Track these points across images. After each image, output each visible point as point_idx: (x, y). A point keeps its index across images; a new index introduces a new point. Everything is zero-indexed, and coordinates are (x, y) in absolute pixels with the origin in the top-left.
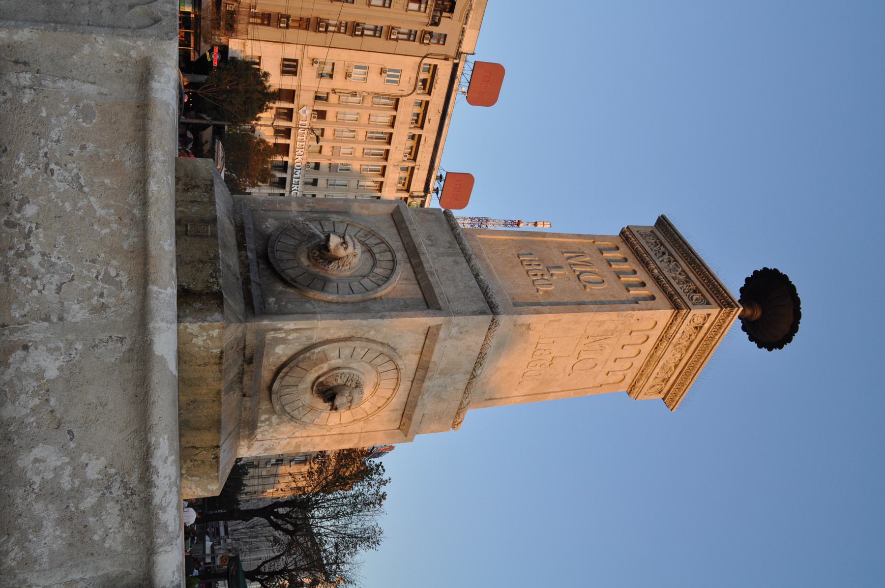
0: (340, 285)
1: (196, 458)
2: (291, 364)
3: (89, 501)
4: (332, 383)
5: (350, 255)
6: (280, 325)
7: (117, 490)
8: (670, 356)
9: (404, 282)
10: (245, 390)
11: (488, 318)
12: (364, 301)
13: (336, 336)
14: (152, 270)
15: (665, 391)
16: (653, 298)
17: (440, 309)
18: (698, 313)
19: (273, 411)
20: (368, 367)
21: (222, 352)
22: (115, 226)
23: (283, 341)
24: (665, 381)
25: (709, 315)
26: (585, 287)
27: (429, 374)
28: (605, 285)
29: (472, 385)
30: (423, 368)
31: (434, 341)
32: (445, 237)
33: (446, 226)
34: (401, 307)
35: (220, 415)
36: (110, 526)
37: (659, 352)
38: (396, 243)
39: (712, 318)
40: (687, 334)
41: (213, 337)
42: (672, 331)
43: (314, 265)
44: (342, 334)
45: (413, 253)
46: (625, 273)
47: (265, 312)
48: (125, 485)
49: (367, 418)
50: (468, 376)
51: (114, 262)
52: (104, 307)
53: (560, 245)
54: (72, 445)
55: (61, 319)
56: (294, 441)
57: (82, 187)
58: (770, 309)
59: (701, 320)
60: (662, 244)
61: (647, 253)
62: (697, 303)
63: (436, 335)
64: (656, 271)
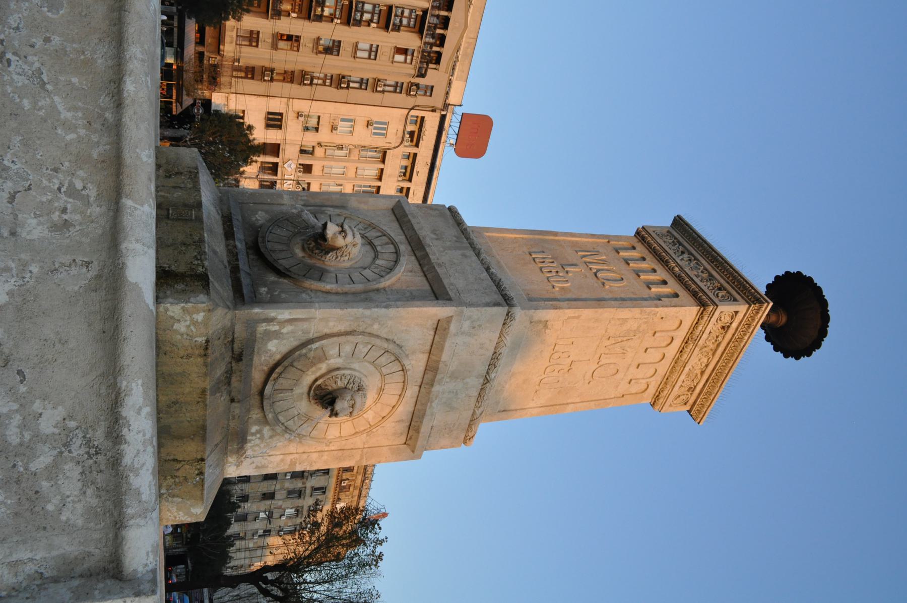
0: (339, 276)
1: (177, 474)
2: (286, 363)
3: (43, 460)
4: (332, 386)
5: (350, 247)
6: (272, 313)
7: (78, 449)
8: (696, 360)
9: (410, 274)
10: (233, 394)
11: (503, 310)
12: (366, 292)
13: (335, 330)
14: (126, 181)
15: (691, 402)
16: (676, 295)
17: (450, 299)
18: (725, 309)
19: (265, 421)
20: (372, 368)
21: (207, 341)
22: (82, 132)
23: (277, 335)
24: (691, 390)
25: (736, 312)
26: (603, 284)
27: (439, 377)
28: (625, 283)
29: (485, 396)
30: (432, 369)
31: (444, 338)
32: (452, 232)
33: (451, 221)
34: (409, 297)
35: (204, 420)
36: (68, 493)
37: (685, 356)
38: (399, 237)
39: (740, 316)
40: (714, 335)
41: (197, 322)
42: (697, 332)
43: (310, 256)
44: (342, 327)
45: (417, 247)
46: (645, 271)
47: (256, 300)
48: (88, 442)
49: (370, 429)
50: (481, 381)
51: (81, 173)
52: (67, 224)
53: (574, 245)
54: (23, 389)
55: (13, 234)
56: (289, 458)
57: (45, 84)
58: (797, 315)
59: (728, 319)
60: (680, 244)
61: (665, 251)
62: (724, 299)
63: (446, 329)
64: (677, 269)
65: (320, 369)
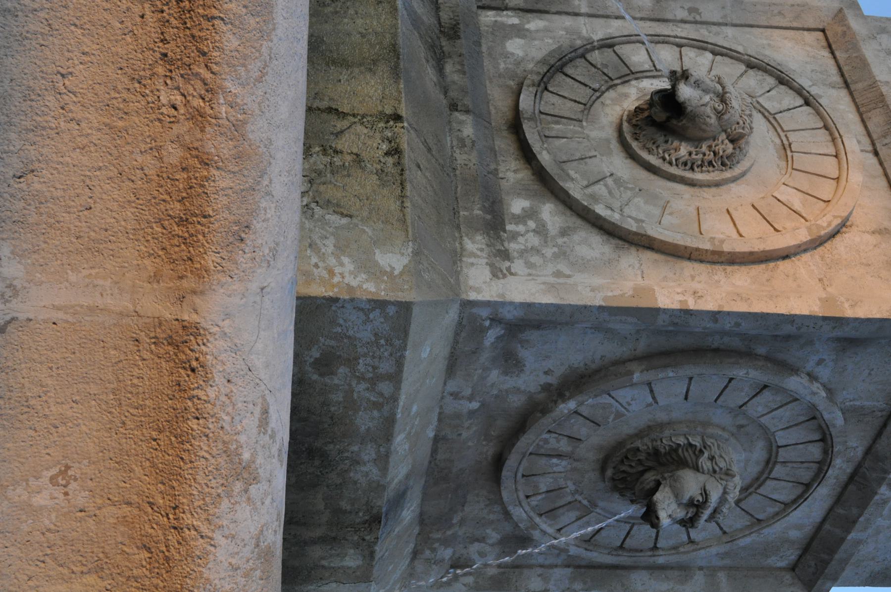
35: (395, 35)
63: (847, 32)
65: (626, 96)
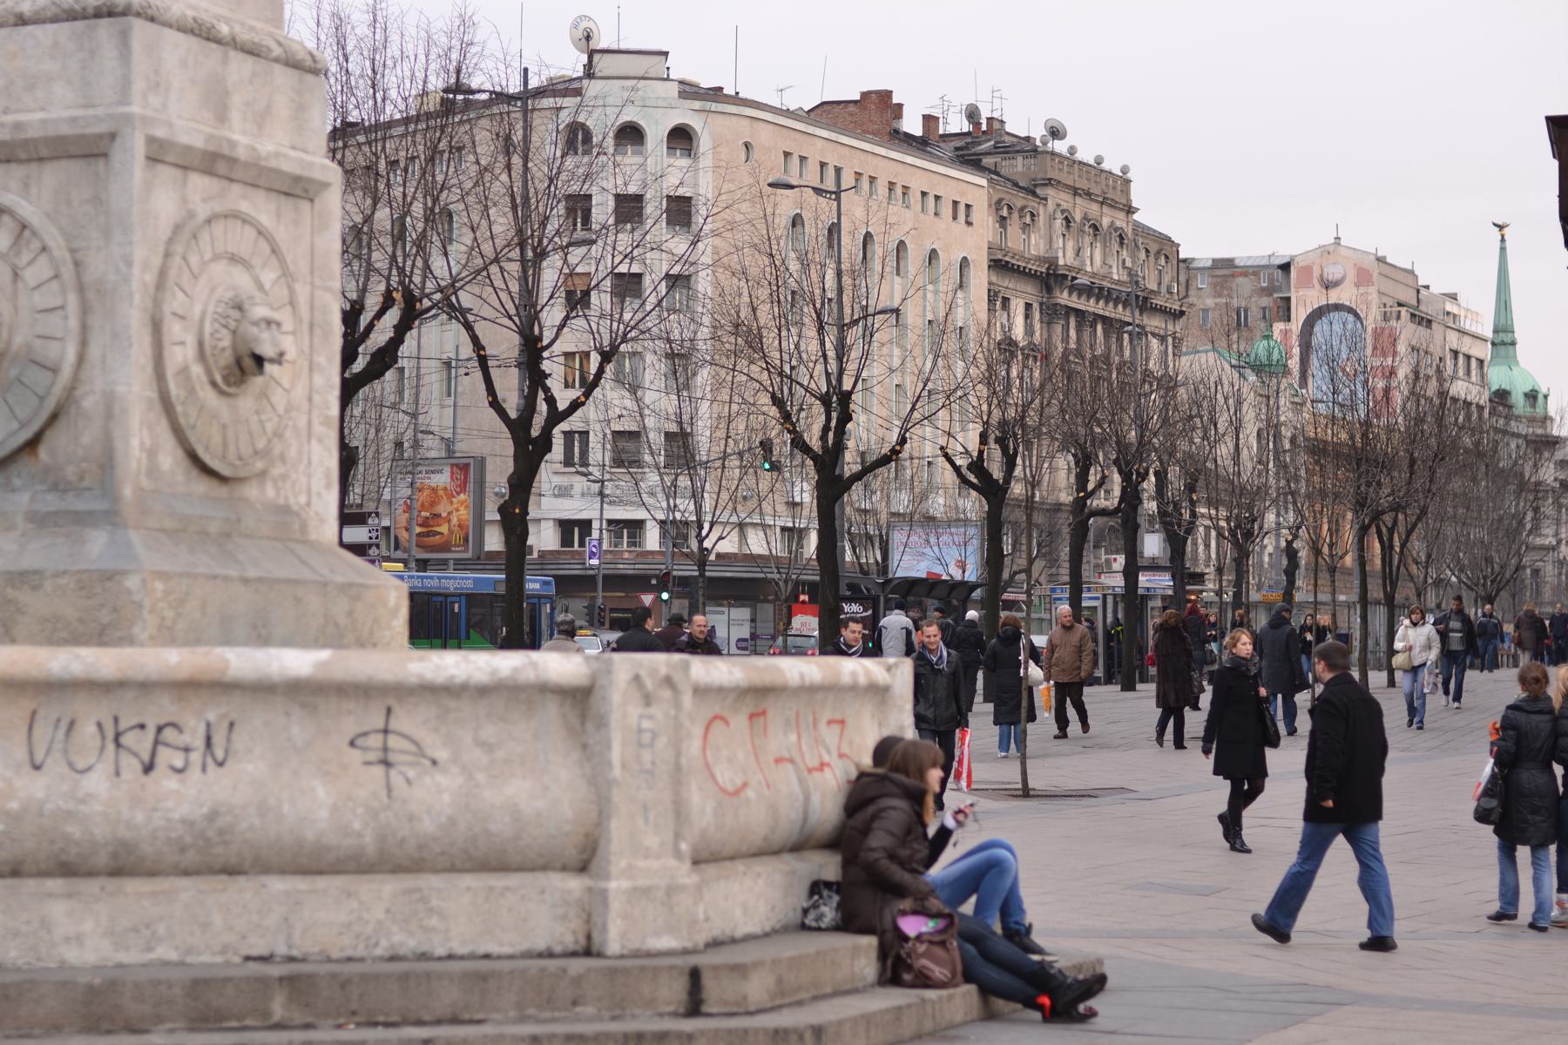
0: (40, 330)
4: (227, 358)
9: (34, 190)
17: (113, 136)
20: (203, 281)
27: (226, 151)
50: (232, 54)
